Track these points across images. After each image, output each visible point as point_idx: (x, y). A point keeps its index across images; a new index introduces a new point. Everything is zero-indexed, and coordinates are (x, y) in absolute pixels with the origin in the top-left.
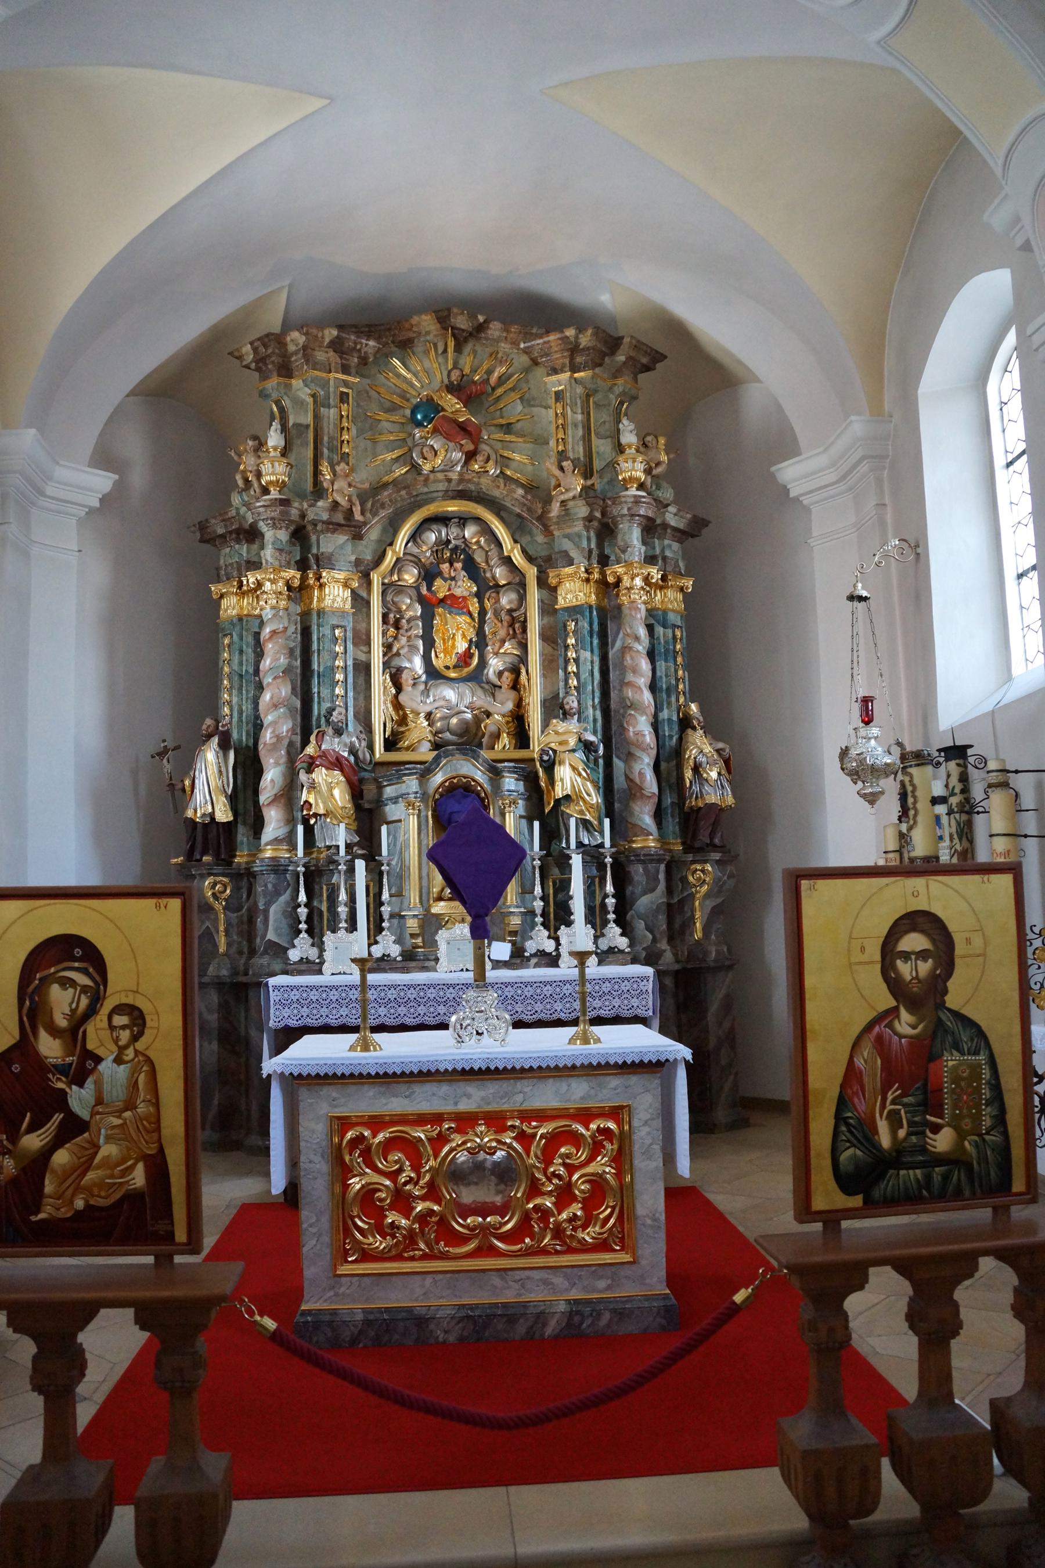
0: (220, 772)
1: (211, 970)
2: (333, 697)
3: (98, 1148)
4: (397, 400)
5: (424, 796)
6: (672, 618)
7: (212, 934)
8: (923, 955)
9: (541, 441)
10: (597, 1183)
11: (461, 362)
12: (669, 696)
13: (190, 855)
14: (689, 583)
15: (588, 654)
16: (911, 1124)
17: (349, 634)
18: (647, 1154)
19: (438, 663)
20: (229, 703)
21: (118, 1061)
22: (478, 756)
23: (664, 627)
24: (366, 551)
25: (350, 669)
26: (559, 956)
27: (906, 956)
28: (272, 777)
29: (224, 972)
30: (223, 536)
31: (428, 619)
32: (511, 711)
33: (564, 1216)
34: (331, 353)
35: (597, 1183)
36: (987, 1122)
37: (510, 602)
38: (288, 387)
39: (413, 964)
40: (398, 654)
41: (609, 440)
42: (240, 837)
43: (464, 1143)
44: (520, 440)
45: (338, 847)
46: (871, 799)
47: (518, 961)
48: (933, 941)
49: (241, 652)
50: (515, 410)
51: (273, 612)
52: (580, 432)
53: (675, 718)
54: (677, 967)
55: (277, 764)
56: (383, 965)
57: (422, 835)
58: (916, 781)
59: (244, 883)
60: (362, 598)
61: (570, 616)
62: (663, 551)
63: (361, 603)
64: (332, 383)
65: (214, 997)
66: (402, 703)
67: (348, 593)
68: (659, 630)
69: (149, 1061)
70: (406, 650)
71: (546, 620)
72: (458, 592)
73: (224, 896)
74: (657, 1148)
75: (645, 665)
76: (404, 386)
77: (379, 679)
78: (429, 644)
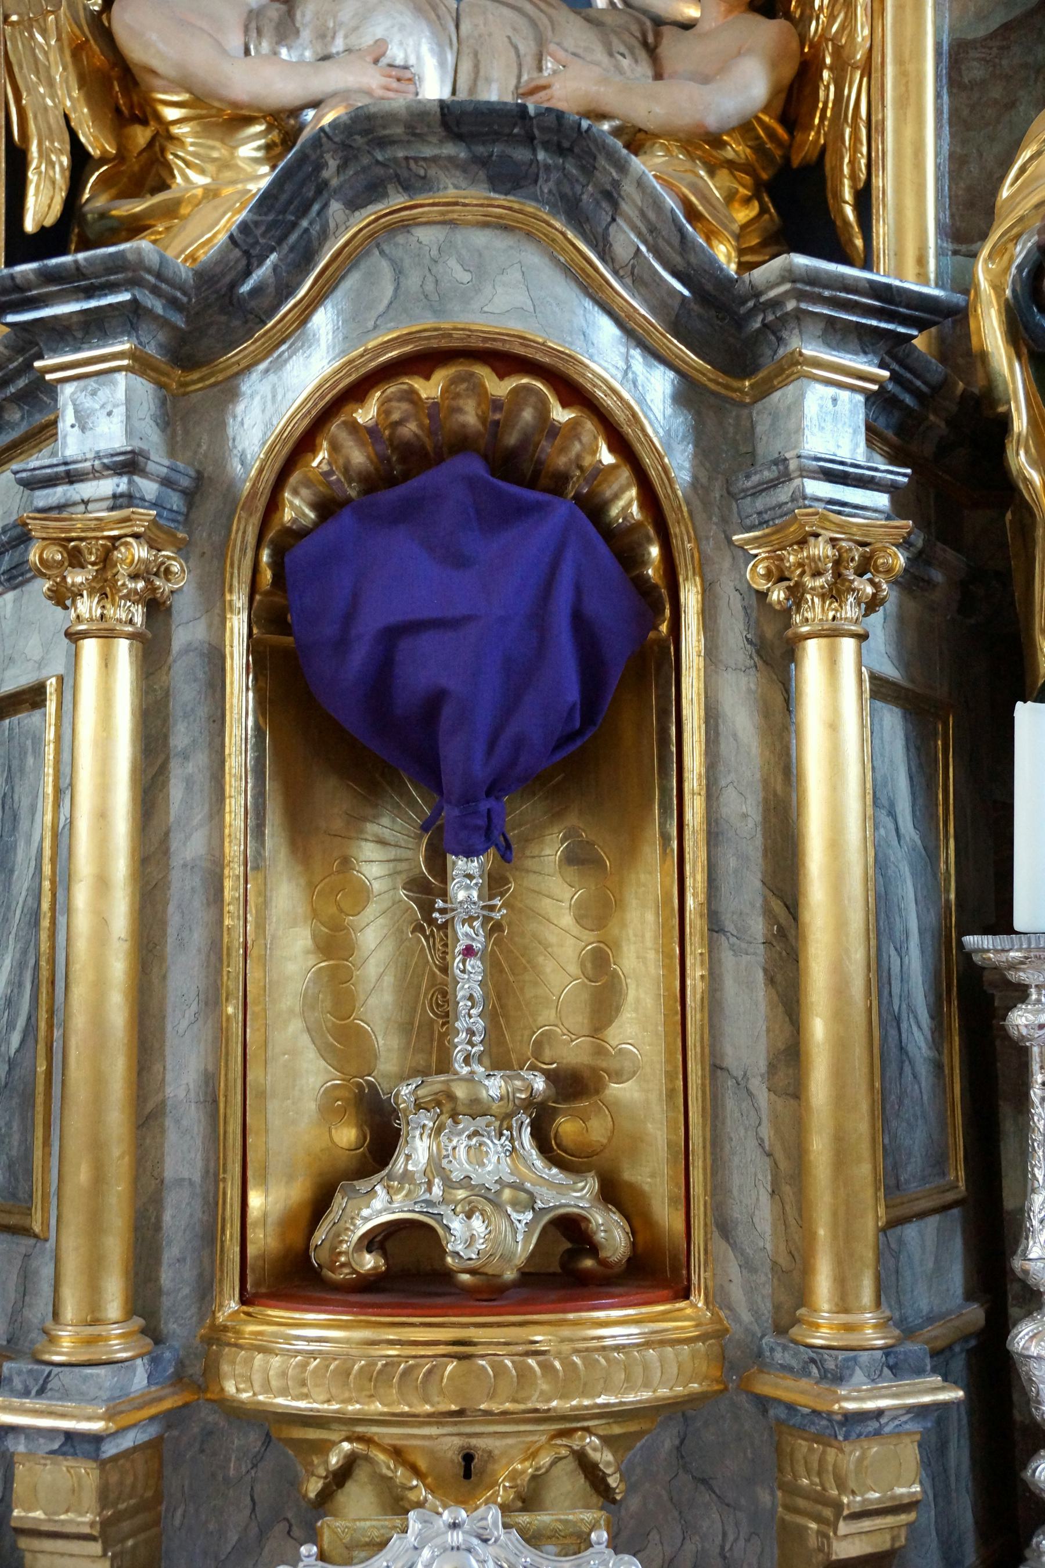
22: (611, 197)
32: (745, 128)
57: (176, 791)
66: (135, 51)
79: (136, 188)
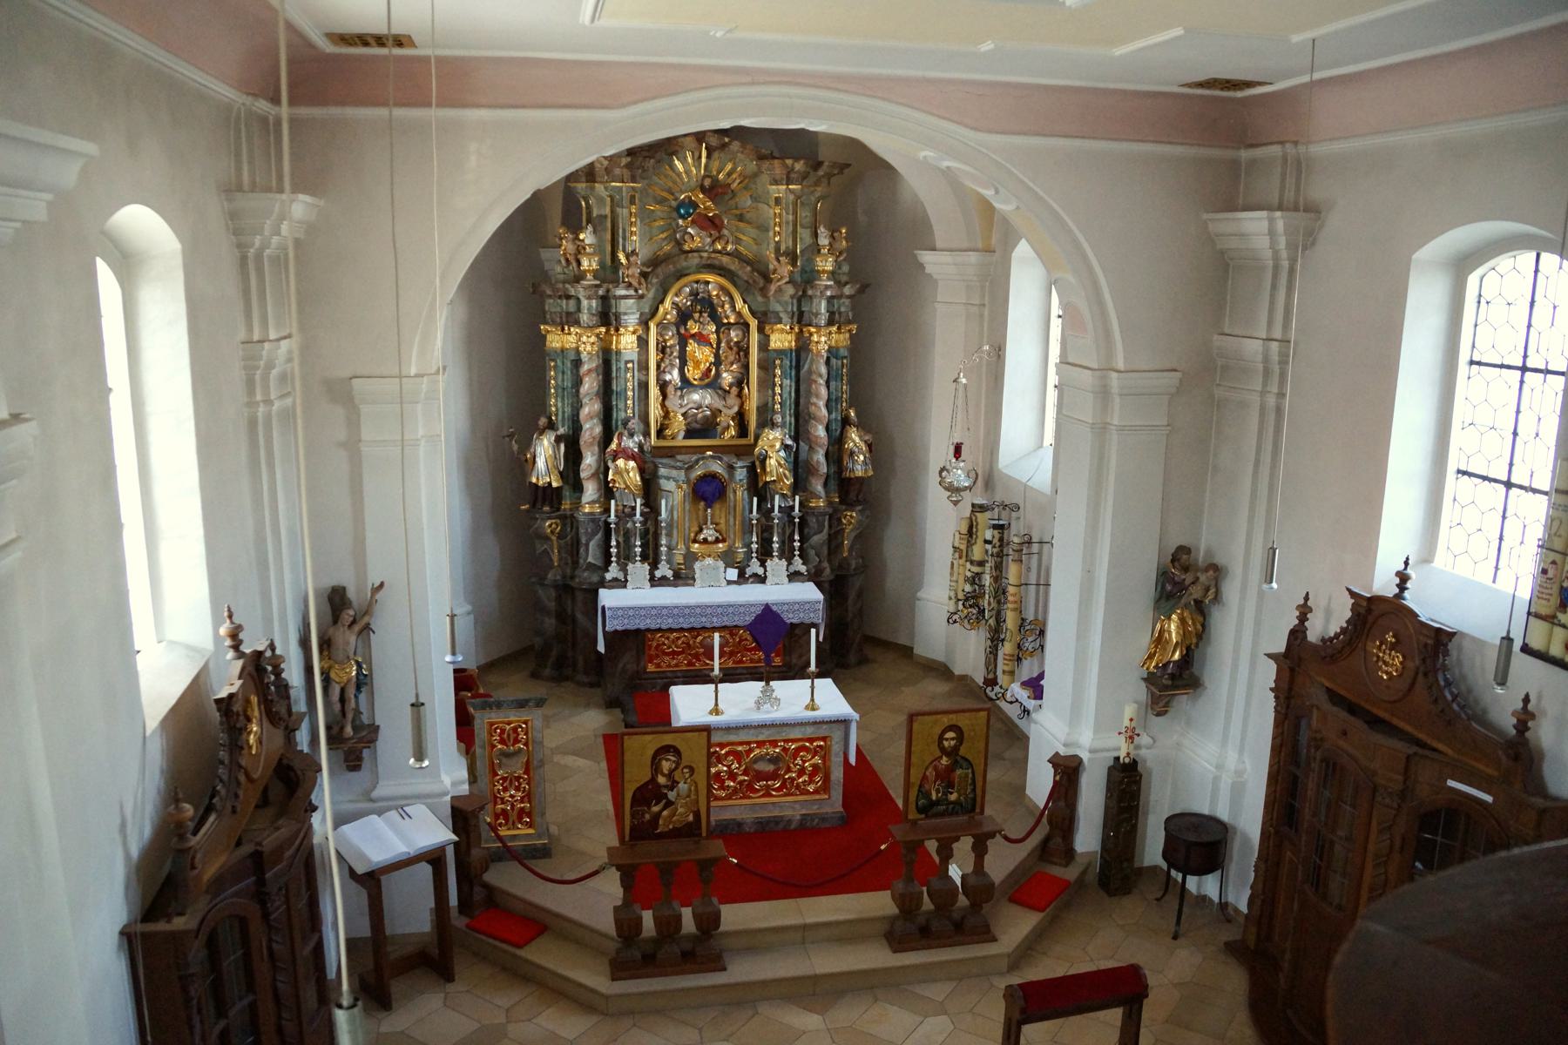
0: (556, 458)
3: (677, 810)
4: (665, 194)
5: (688, 481)
6: (843, 352)
7: (548, 553)
8: (953, 739)
9: (764, 228)
10: (815, 766)
11: (711, 166)
12: (837, 404)
13: (534, 505)
14: (854, 327)
15: (788, 381)
16: (943, 792)
17: (636, 366)
18: (837, 755)
19: (689, 375)
20: (556, 406)
21: (685, 783)
23: (837, 358)
25: (636, 388)
26: (766, 577)
27: (947, 739)
28: (589, 460)
29: (558, 577)
31: (683, 343)
33: (800, 780)
34: (625, 170)
35: (815, 766)
36: (969, 790)
37: (737, 336)
38: (593, 189)
39: (681, 582)
40: (664, 372)
41: (809, 230)
45: (634, 508)
46: (956, 503)
47: (742, 580)
48: (957, 734)
49: (563, 373)
50: (745, 201)
51: (589, 356)
52: (791, 228)
53: (839, 418)
56: (663, 582)
58: (979, 520)
59: (569, 521)
60: (643, 339)
61: (777, 355)
62: (839, 308)
63: (643, 343)
64: (624, 189)
65: (553, 593)
67: (634, 338)
68: (834, 361)
69: (695, 783)
70: (669, 367)
71: (761, 355)
72: (704, 332)
74: (841, 754)
75: (823, 391)
76: (671, 184)
77: (654, 391)
78: (683, 363)
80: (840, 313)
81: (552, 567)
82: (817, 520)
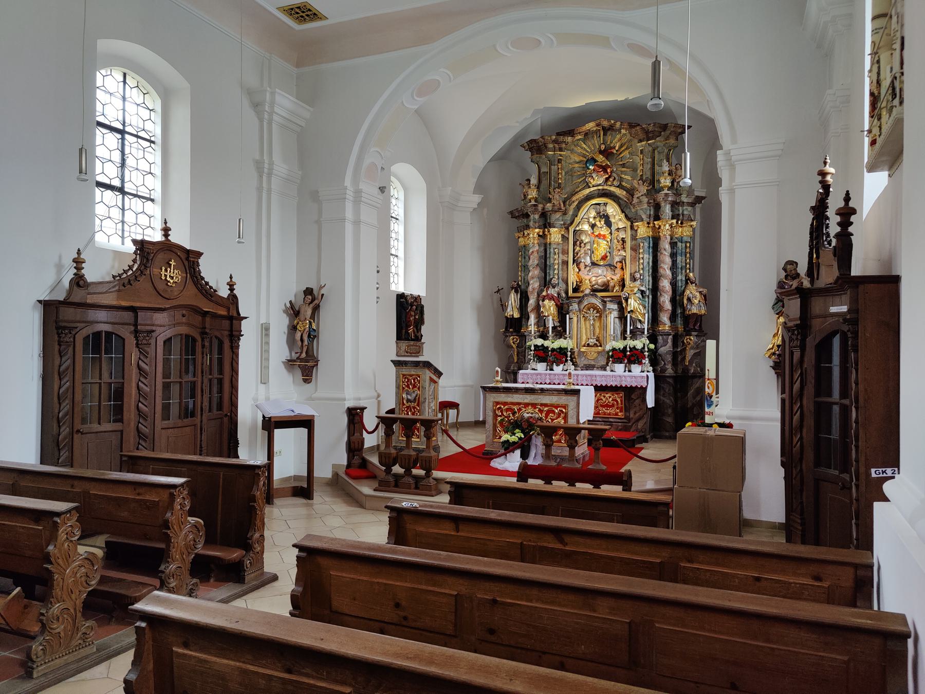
1: (512, 368)
2: (554, 274)
6: (685, 239)
12: (682, 270)
17: (560, 251)
20: (521, 276)
24: (568, 218)
28: (532, 302)
30: (518, 216)
42: (523, 323)
43: (526, 411)
44: (628, 170)
53: (684, 279)
54: (675, 375)
55: (533, 298)
63: (565, 238)
67: (560, 236)
73: (516, 343)
74: (575, 416)
75: (668, 260)
76: (584, 152)
79: (580, 283)
80: (683, 215)
81: (513, 362)
82: (663, 339)
